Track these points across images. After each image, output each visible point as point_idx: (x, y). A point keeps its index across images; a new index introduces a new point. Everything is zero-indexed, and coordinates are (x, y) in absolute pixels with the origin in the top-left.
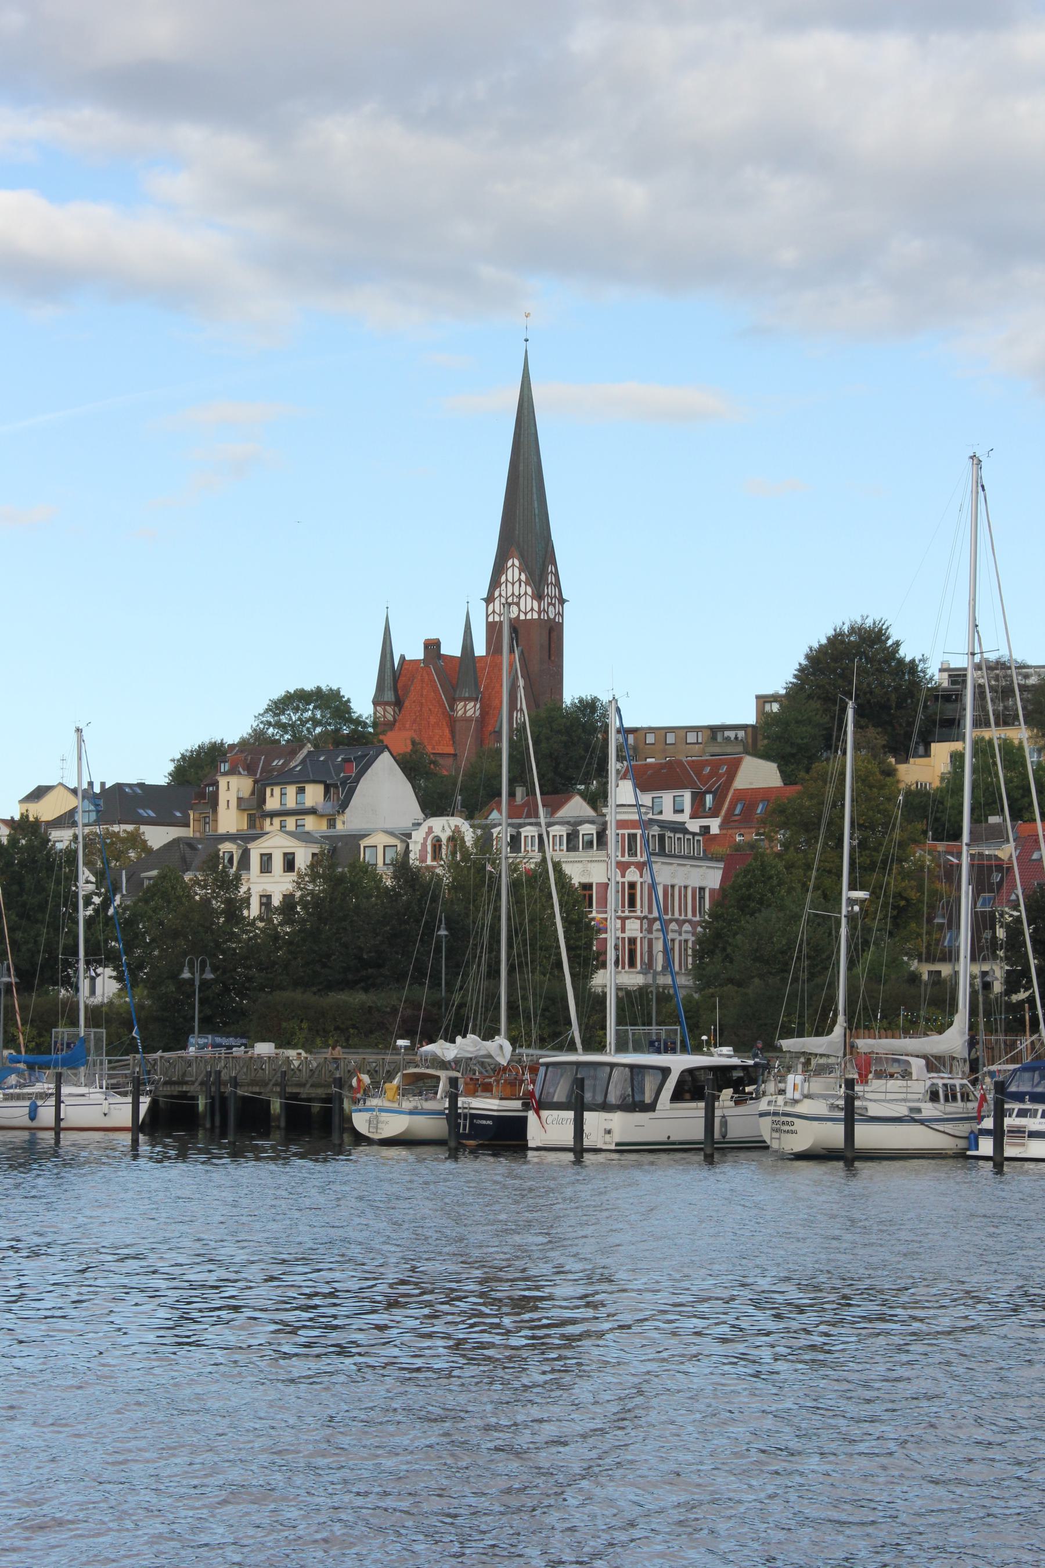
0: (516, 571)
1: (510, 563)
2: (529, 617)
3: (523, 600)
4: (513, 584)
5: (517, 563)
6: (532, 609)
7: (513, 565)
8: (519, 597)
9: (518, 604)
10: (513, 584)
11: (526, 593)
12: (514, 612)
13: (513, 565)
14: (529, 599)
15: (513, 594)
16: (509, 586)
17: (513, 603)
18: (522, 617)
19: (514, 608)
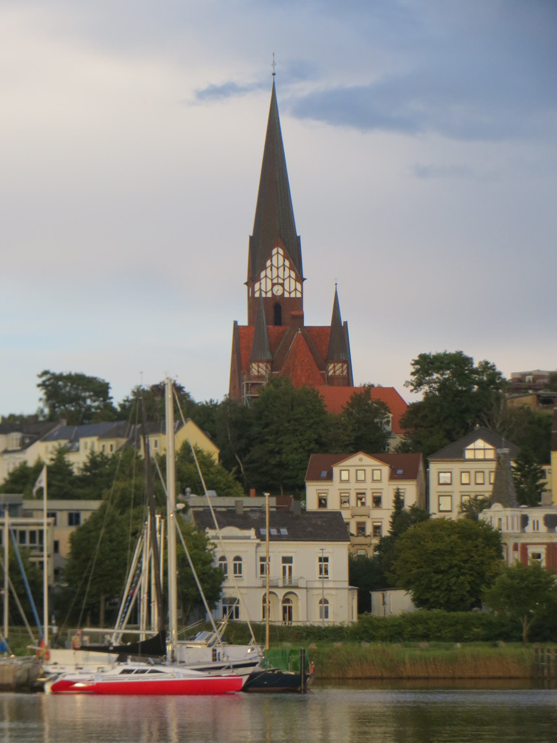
0: (281, 258)
1: (274, 251)
2: (293, 295)
3: (287, 282)
4: (278, 268)
5: (281, 251)
6: (296, 289)
7: (278, 253)
8: (284, 280)
9: (282, 285)
10: (278, 268)
11: (290, 276)
12: (278, 290)
13: (278, 253)
14: (293, 281)
15: (278, 276)
16: (274, 269)
17: (278, 284)
18: (287, 295)
19: (280, 288)
